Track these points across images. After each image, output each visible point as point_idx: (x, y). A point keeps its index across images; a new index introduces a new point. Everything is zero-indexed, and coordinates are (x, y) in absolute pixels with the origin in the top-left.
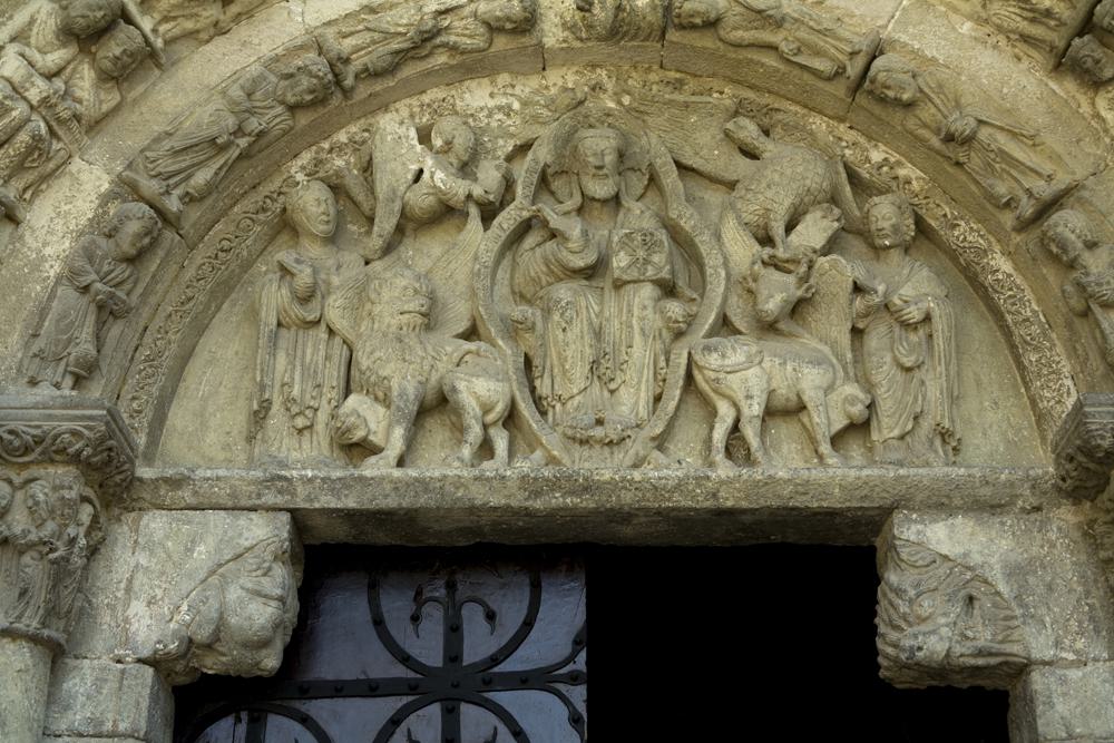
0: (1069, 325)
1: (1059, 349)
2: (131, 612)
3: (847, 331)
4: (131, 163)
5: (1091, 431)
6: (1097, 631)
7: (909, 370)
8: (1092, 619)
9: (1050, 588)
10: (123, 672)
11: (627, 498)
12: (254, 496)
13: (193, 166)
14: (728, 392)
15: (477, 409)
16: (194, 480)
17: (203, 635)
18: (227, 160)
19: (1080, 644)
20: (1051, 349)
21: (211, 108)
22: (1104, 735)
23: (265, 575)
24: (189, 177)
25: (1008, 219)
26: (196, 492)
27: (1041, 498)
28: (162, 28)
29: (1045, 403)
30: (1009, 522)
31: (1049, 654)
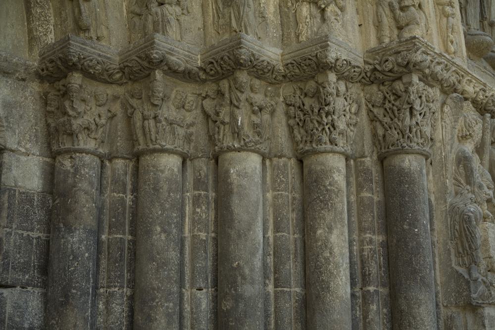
1: (51, 11)
5: (71, 52)
6: (37, 142)
8: (36, 136)
9: (21, 117)
19: (28, 146)
20: (48, 10)
22: (30, 188)
27: (27, 75)
29: (38, 33)
30: (10, 82)
31: (14, 147)
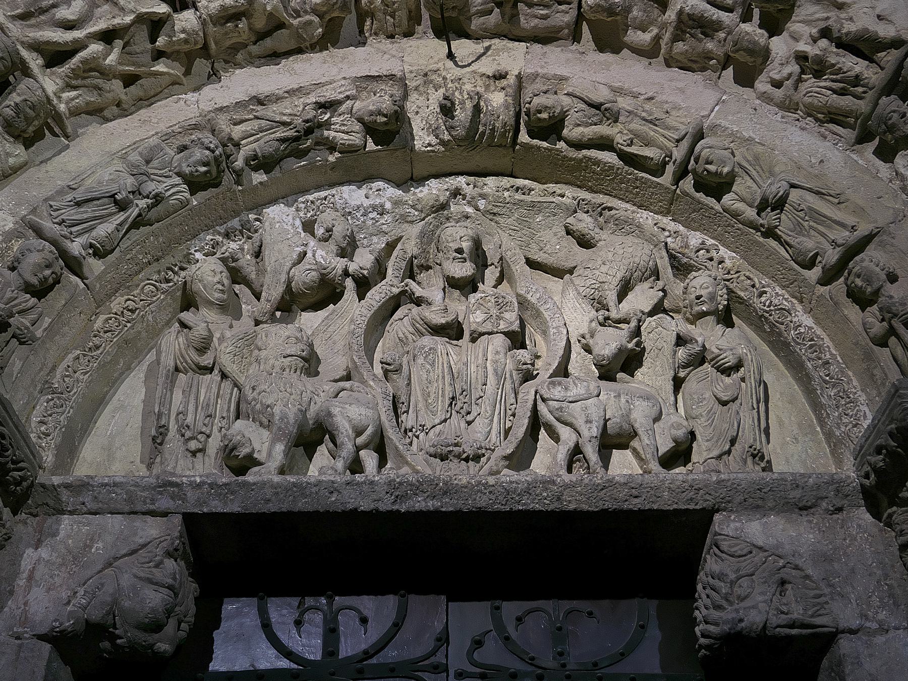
0: (868, 356)
2: (31, 597)
3: (671, 378)
4: (35, 209)
7: (724, 403)
10: (20, 646)
11: (482, 501)
12: (148, 501)
13: (95, 218)
14: (570, 419)
15: (350, 432)
16: (93, 486)
17: (96, 615)
18: (128, 217)
21: (112, 169)
23: (157, 566)
24: (92, 228)
25: (814, 274)
26: (96, 498)
28: (66, 95)
